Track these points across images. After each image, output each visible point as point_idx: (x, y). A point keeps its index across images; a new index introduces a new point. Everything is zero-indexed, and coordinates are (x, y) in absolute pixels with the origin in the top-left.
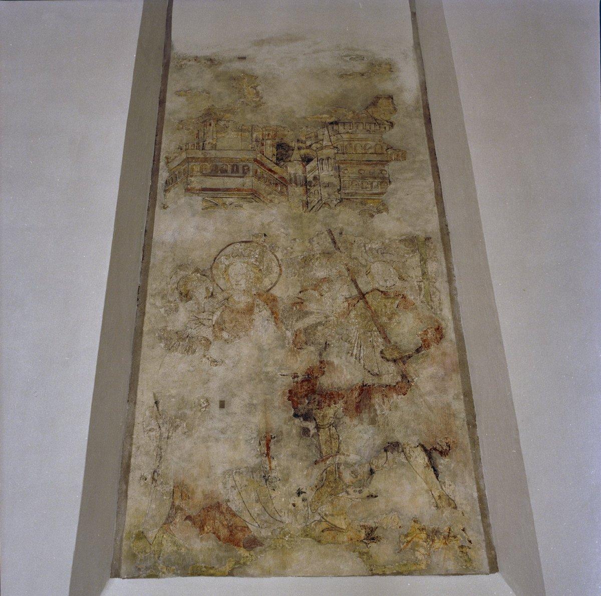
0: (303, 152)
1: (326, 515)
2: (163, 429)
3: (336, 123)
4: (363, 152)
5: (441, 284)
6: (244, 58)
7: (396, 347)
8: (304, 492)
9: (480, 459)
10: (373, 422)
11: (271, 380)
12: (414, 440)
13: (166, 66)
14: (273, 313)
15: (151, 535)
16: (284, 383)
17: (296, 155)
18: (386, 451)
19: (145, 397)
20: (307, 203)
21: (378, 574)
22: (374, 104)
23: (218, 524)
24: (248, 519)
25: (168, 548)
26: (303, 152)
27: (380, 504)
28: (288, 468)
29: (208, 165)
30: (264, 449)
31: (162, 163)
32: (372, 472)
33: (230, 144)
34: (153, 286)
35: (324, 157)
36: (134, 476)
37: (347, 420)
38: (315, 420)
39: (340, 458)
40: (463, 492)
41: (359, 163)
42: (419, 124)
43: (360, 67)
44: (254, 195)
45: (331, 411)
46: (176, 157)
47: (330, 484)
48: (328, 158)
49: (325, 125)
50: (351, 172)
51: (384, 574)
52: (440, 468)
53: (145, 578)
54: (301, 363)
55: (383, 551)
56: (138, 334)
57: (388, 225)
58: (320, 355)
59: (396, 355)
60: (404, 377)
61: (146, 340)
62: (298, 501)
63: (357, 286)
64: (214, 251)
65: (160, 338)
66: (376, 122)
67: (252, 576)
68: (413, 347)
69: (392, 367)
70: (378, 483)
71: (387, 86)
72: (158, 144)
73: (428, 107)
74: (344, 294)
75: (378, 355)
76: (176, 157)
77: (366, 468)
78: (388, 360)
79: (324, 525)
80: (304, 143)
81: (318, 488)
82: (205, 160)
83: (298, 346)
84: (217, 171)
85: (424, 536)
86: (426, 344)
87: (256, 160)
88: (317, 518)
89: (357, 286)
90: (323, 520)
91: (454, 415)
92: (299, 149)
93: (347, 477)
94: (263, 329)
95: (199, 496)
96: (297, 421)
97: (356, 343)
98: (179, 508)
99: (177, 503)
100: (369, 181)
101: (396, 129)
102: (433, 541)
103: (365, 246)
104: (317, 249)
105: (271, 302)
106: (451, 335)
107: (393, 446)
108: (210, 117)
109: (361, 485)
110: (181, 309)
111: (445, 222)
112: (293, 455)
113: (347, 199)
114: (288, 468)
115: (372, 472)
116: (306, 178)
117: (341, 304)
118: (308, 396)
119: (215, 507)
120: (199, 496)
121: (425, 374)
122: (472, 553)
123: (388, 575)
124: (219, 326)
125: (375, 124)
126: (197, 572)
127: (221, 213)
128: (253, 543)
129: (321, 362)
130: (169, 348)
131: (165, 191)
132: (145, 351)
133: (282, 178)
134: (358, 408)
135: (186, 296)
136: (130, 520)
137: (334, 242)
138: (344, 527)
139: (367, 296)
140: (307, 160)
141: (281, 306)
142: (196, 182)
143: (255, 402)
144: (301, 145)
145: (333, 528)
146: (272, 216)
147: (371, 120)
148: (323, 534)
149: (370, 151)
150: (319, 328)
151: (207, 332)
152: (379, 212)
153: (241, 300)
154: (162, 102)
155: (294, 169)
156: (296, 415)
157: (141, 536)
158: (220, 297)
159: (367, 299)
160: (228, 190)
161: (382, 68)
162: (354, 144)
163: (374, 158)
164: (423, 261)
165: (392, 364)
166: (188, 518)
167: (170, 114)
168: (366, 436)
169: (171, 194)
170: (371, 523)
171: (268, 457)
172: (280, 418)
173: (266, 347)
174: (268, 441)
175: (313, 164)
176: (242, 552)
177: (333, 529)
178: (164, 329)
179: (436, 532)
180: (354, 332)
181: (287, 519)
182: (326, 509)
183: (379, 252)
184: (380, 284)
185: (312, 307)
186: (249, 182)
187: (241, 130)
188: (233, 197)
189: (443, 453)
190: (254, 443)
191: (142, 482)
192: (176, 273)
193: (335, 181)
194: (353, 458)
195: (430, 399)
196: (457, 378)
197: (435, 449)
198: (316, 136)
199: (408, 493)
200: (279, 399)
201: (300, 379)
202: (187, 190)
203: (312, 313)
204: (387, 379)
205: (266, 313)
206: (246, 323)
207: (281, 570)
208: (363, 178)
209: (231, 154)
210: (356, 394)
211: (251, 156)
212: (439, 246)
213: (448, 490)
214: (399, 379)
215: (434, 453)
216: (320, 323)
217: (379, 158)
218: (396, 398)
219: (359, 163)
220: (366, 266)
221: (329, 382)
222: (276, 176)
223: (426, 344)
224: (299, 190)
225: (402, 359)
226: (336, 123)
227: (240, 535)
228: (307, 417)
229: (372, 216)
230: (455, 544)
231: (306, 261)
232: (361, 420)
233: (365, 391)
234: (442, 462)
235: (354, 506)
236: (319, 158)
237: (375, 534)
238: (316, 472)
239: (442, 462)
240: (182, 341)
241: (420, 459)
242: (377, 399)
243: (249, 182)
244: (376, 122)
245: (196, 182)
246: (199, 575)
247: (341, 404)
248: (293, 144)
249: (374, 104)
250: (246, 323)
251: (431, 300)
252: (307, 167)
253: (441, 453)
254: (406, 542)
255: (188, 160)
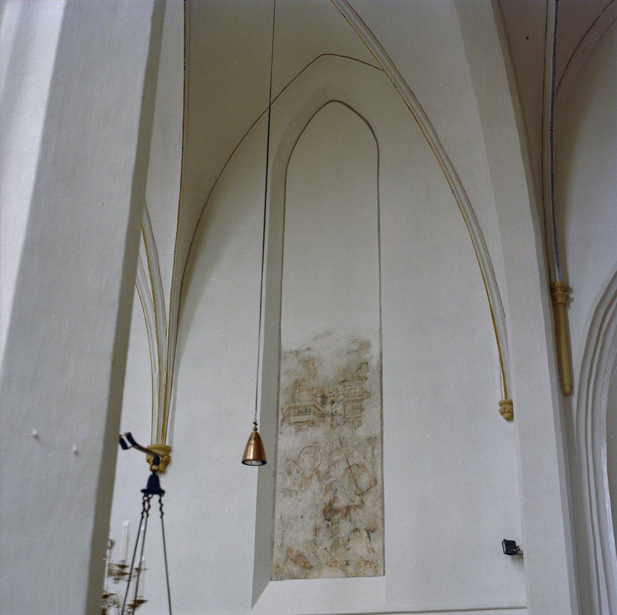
0: (331, 398)
3: (344, 381)
5: (378, 460)
6: (309, 349)
7: (360, 489)
10: (350, 521)
11: (317, 506)
12: (363, 527)
13: (280, 358)
14: (319, 478)
15: (281, 566)
16: (322, 507)
17: (329, 401)
19: (277, 516)
20: (332, 425)
22: (360, 368)
23: (300, 561)
24: (309, 559)
25: (286, 570)
26: (331, 398)
27: (351, 552)
28: (322, 540)
29: (296, 410)
30: (315, 534)
31: (280, 412)
32: (349, 540)
33: (305, 399)
34: (279, 470)
35: (339, 400)
36: (276, 545)
37: (342, 520)
39: (339, 535)
40: (377, 546)
41: (353, 401)
42: (377, 377)
43: (356, 347)
44: (313, 423)
45: (337, 517)
47: (335, 545)
48: (341, 401)
49: (340, 383)
50: (349, 407)
51: (350, 577)
52: (371, 537)
54: (327, 499)
55: (350, 569)
56: (275, 490)
57: (361, 433)
58: (334, 494)
59: (360, 492)
60: (362, 502)
61: (277, 492)
62: (325, 552)
63: (348, 463)
64: (299, 452)
65: (282, 492)
66: (360, 378)
67: (311, 579)
68: (366, 489)
69: (358, 498)
70: (351, 544)
71: (366, 357)
72: (278, 401)
77: (347, 539)
78: (357, 495)
81: (331, 547)
82: (296, 407)
83: (327, 491)
84: (300, 413)
85: (363, 563)
86: (371, 487)
87: (314, 405)
89: (348, 463)
91: (378, 517)
93: (341, 542)
94: (315, 485)
95: (295, 552)
96: (326, 522)
98: (289, 556)
99: (288, 554)
101: (368, 382)
104: (335, 447)
105: (318, 472)
106: (380, 482)
107: (356, 530)
108: (297, 385)
109: (345, 545)
110: (288, 479)
112: (324, 535)
114: (322, 540)
115: (349, 540)
116: (332, 412)
117: (342, 471)
118: (329, 512)
119: (300, 555)
120: (295, 552)
121: (369, 499)
122: (378, 569)
124: (301, 485)
126: (295, 578)
127: (301, 433)
128: (311, 568)
129: (334, 498)
130: (285, 496)
131: (281, 425)
132: (277, 497)
133: (323, 413)
134: (346, 516)
135: (290, 473)
136: (274, 561)
137: (341, 443)
140: (333, 402)
141: (322, 474)
142: (293, 419)
143: (312, 515)
144: (331, 395)
145: (336, 561)
146: (318, 433)
147: (358, 378)
148: (332, 564)
149: (358, 395)
150: (334, 483)
151: (297, 488)
152: (358, 426)
153: (308, 473)
154: (279, 379)
155: (328, 408)
156: (325, 520)
157: (278, 566)
158: (301, 472)
160: (303, 422)
161: (365, 346)
162: (351, 391)
163: (359, 398)
164: (373, 448)
165: (358, 496)
166: (292, 560)
167: (282, 385)
168: (348, 527)
169: (283, 426)
170: (347, 559)
172: (320, 521)
173: (316, 493)
174: (316, 530)
175: (335, 404)
176: (308, 571)
178: (283, 488)
179: (368, 561)
180: (346, 485)
181: (322, 559)
182: (333, 554)
184: (357, 461)
185: (332, 474)
186: (311, 417)
187: (309, 390)
189: (372, 532)
190: (312, 531)
191: (278, 548)
192: (286, 463)
193: (342, 412)
194: (343, 535)
195: (370, 510)
196: (380, 501)
197: (370, 530)
198: (337, 389)
199: (360, 548)
200: (320, 514)
201: (327, 505)
202: (289, 424)
204: (356, 503)
205: (316, 478)
206: (310, 483)
207: (319, 577)
208: (354, 409)
209: (304, 403)
210: (345, 510)
211: (312, 403)
212: (380, 441)
213: (373, 546)
214: (360, 503)
215: (370, 531)
216: (334, 481)
217: (360, 398)
218: (359, 511)
219: (353, 401)
220: (351, 453)
221: (336, 505)
222: (321, 413)
223: (371, 487)
224: (328, 419)
225: (362, 494)
226: (344, 381)
227: (307, 565)
228: (329, 520)
229: (356, 429)
230: (374, 565)
231: (331, 453)
232: (346, 520)
233: (348, 508)
234: (372, 535)
235: (342, 553)
237: (349, 562)
238: (331, 541)
239: (372, 535)
240: (288, 492)
241: (365, 534)
242: (352, 511)
243: (311, 417)
244: (360, 378)
245: (293, 419)
247: (340, 514)
248: (328, 395)
249: (360, 368)
250: (310, 483)
253: (372, 531)
254: (358, 565)
255: (289, 408)
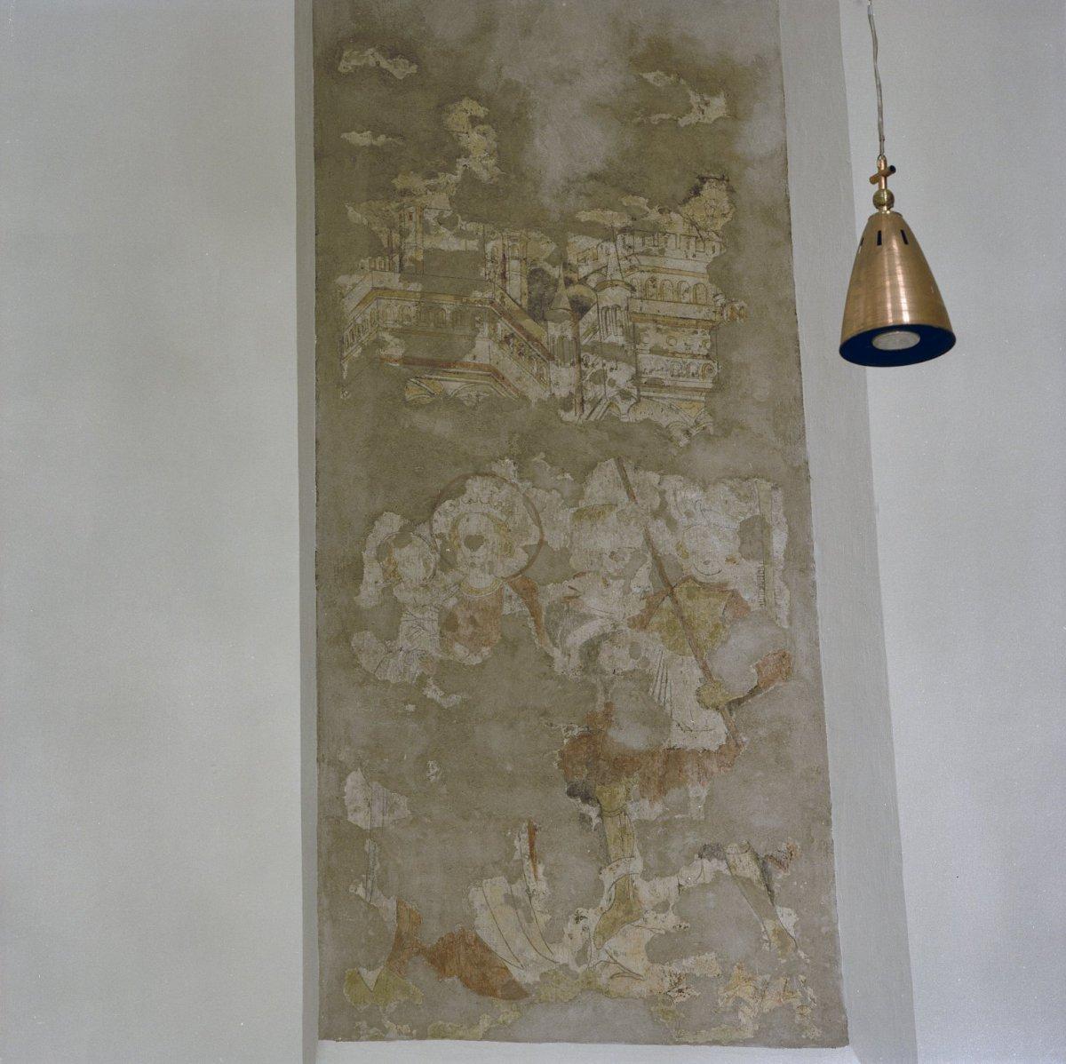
1: (615, 953)
2: (375, 809)
4: (676, 299)
8: (585, 917)
9: (834, 876)
18: (701, 857)
21: (687, 1043)
26: (573, 290)
38: (598, 802)
46: (354, 285)
52: (776, 886)
53: (367, 1040)
59: (720, 698)
73: (788, 206)
74: (641, 584)
75: (693, 697)
76: (354, 285)
79: (613, 969)
80: (575, 272)
88: (605, 957)
90: (612, 961)
92: (569, 282)
97: (660, 674)
100: (684, 363)
102: (763, 997)
103: (675, 494)
111: (805, 455)
113: (648, 397)
123: (701, 1044)
125: (697, 238)
138: (641, 973)
139: (676, 590)
150: (605, 645)
159: (678, 597)
171: (532, 861)
177: (626, 975)
183: (698, 507)
188: (458, 379)
189: (780, 863)
203: (592, 617)
216: (604, 636)
236: (601, 307)
246: (443, 1038)
251: (776, 604)
252: (580, 323)
